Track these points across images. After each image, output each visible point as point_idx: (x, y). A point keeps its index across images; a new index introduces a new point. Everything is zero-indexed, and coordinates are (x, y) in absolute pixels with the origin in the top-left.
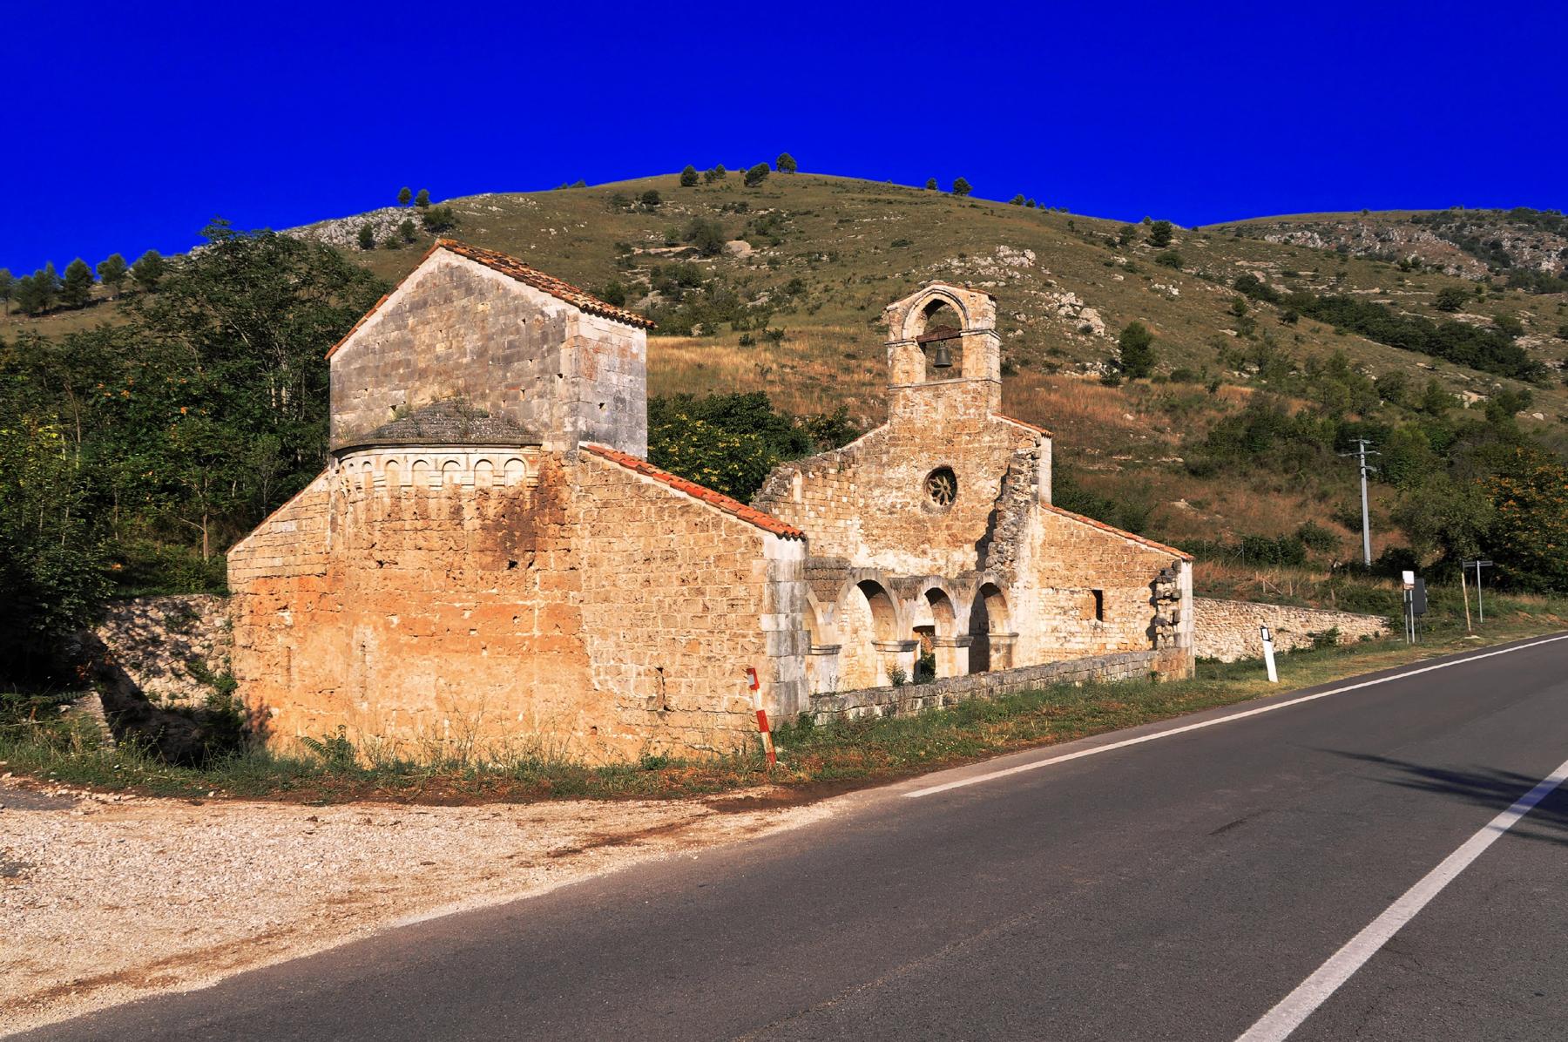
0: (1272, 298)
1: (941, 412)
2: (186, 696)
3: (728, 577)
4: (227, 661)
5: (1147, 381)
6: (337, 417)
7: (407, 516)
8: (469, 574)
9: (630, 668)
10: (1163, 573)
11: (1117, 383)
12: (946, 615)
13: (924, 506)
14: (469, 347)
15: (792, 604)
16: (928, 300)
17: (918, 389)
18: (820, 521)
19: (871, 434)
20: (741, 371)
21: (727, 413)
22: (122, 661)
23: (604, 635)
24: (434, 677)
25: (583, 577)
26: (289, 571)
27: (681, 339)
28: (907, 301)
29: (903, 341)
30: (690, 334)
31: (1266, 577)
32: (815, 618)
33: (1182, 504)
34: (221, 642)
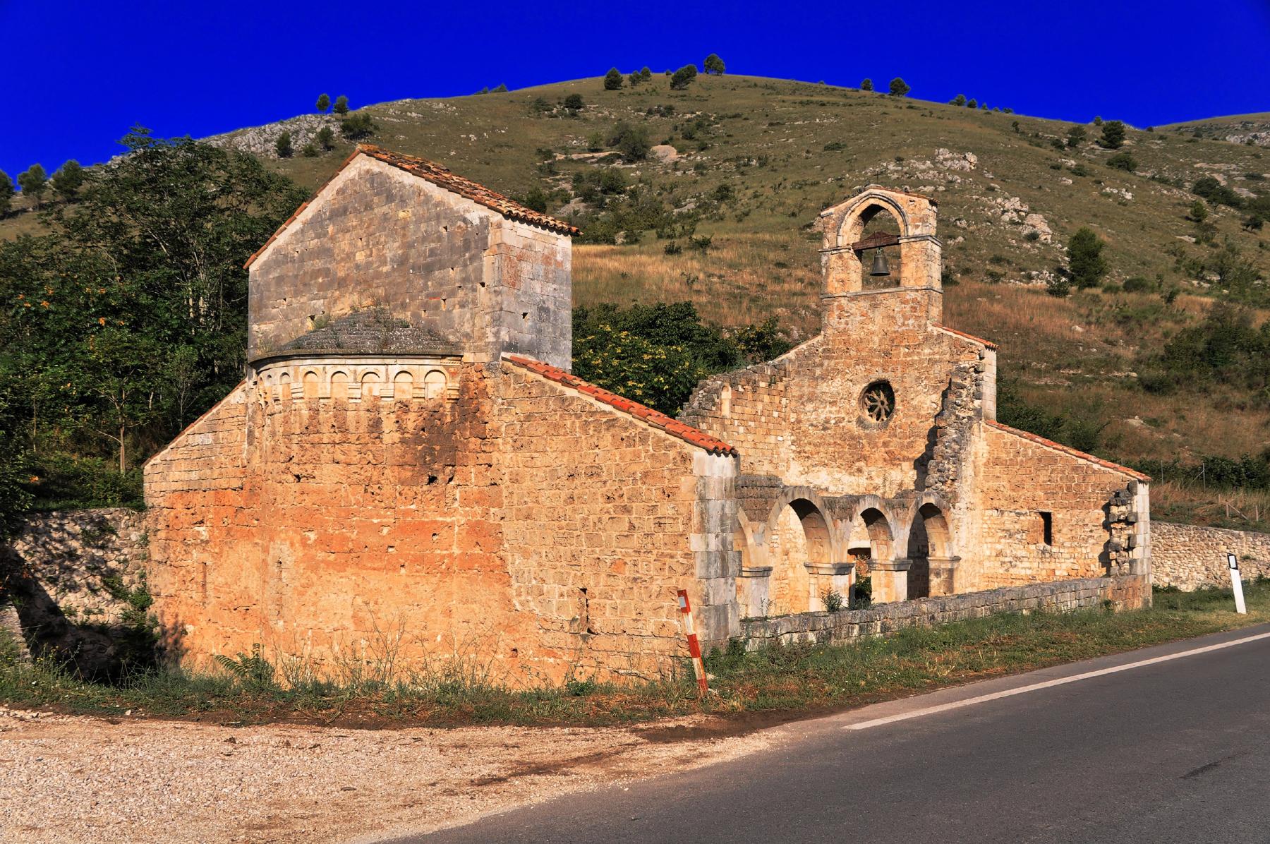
0: (1234, 202)
1: (878, 322)
2: (101, 612)
3: (655, 494)
4: (143, 576)
5: (1097, 291)
6: (255, 327)
7: (325, 428)
8: (388, 489)
9: (553, 588)
10: (1117, 495)
11: (1065, 293)
12: (883, 537)
13: (860, 422)
14: (389, 255)
15: (723, 524)
16: (865, 206)
17: (855, 298)
18: (750, 437)
19: (803, 346)
20: (667, 280)
21: (652, 324)
22: (39, 575)
23: (526, 554)
24: (349, 597)
25: (505, 493)
26: (205, 485)
27: (605, 247)
28: (842, 206)
29: (837, 249)
30: (614, 243)
31: (1231, 500)
32: (745, 539)
33: (1136, 422)
34: (136, 556)
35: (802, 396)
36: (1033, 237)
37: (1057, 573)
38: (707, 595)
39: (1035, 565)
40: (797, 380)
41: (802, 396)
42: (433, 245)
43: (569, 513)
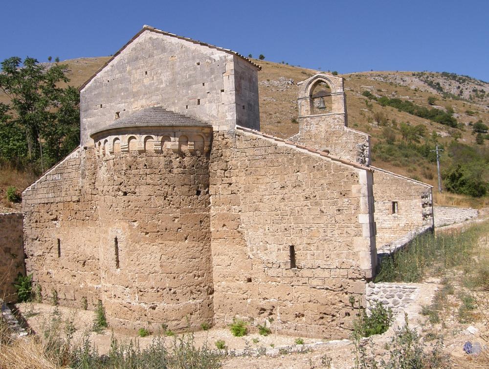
0: (375, 99)
1: (323, 127)
3: (336, 195)
7: (141, 166)
8: (176, 199)
23: (256, 229)
25: (241, 197)
26: (58, 199)
37: (400, 225)
39: (392, 223)
42: (191, 72)
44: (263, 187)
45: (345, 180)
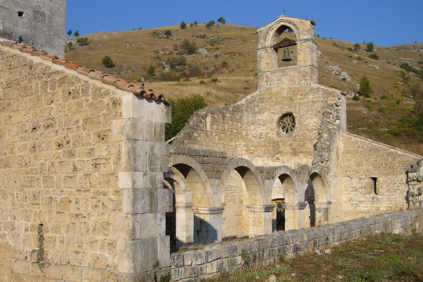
0: (415, 71)
3: (93, 137)
9: (21, 223)
12: (291, 190)
13: (278, 134)
15: (151, 163)
16: (278, 26)
18: (221, 142)
27: (176, 82)
28: (267, 27)
29: (265, 47)
35: (248, 122)
36: (344, 80)
37: (381, 209)
38: (134, 229)
39: (369, 205)
40: (246, 114)
41: (248, 122)
43: (32, 160)
44: (15, 129)
45: (105, 111)
